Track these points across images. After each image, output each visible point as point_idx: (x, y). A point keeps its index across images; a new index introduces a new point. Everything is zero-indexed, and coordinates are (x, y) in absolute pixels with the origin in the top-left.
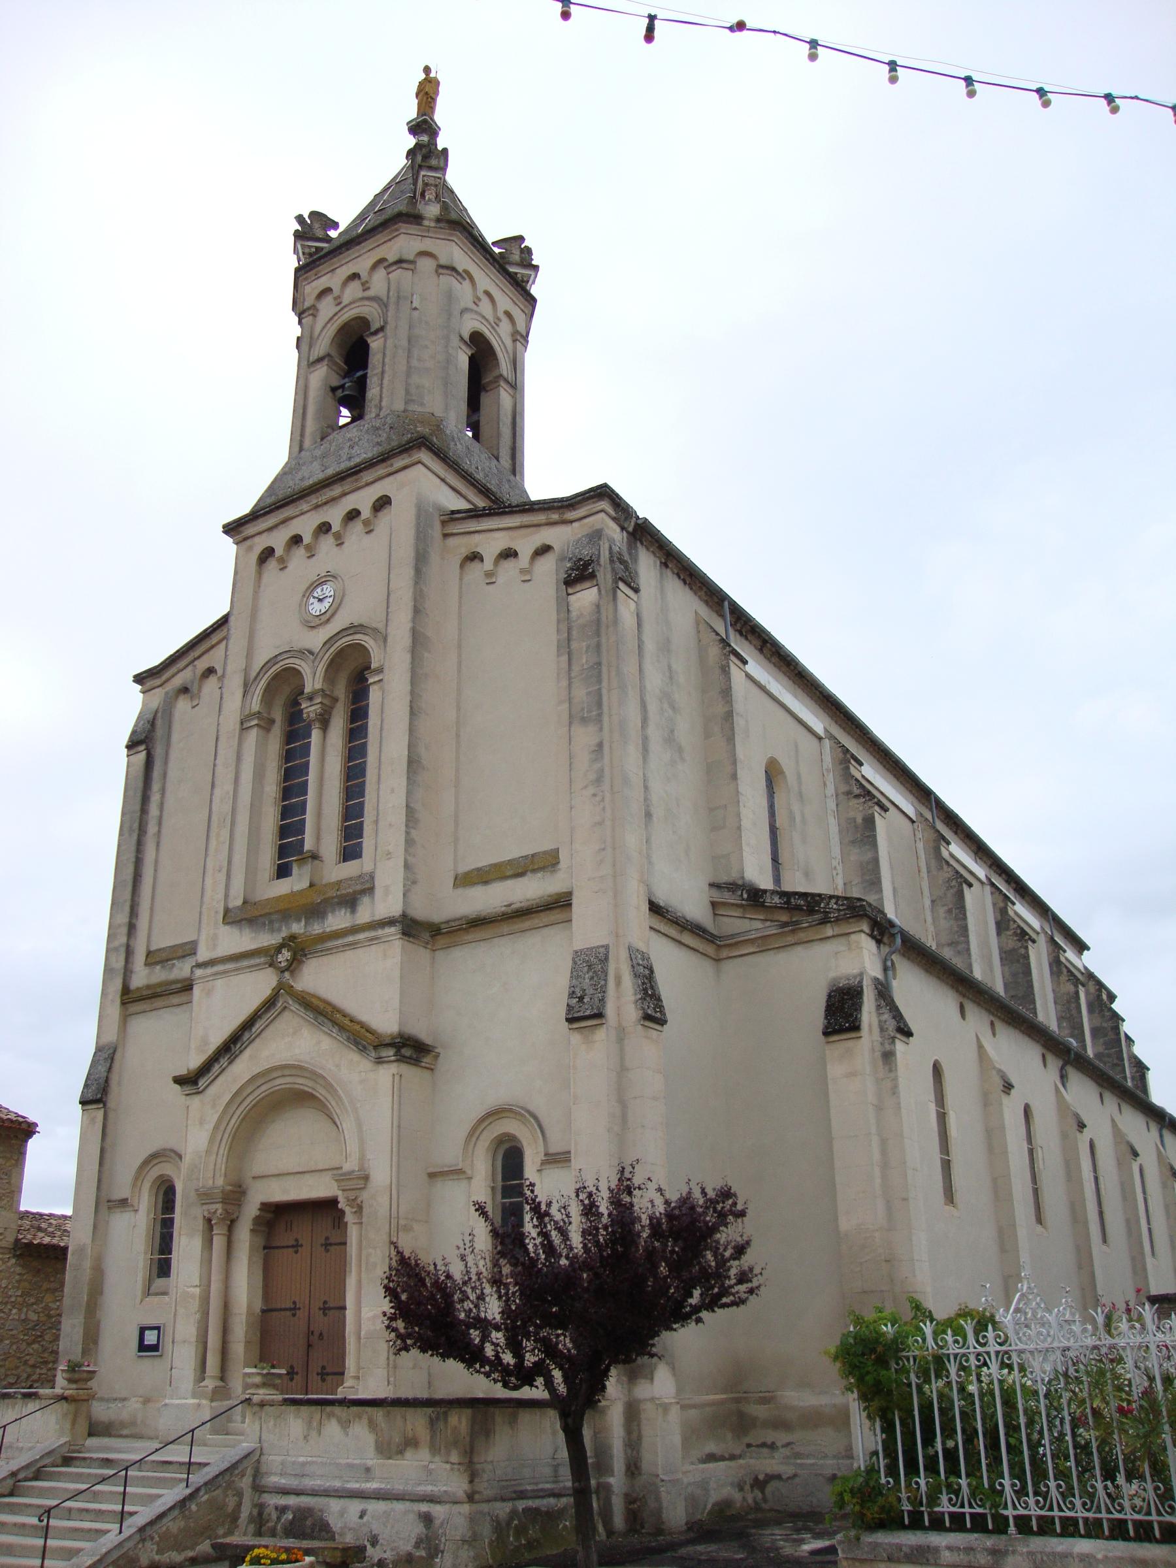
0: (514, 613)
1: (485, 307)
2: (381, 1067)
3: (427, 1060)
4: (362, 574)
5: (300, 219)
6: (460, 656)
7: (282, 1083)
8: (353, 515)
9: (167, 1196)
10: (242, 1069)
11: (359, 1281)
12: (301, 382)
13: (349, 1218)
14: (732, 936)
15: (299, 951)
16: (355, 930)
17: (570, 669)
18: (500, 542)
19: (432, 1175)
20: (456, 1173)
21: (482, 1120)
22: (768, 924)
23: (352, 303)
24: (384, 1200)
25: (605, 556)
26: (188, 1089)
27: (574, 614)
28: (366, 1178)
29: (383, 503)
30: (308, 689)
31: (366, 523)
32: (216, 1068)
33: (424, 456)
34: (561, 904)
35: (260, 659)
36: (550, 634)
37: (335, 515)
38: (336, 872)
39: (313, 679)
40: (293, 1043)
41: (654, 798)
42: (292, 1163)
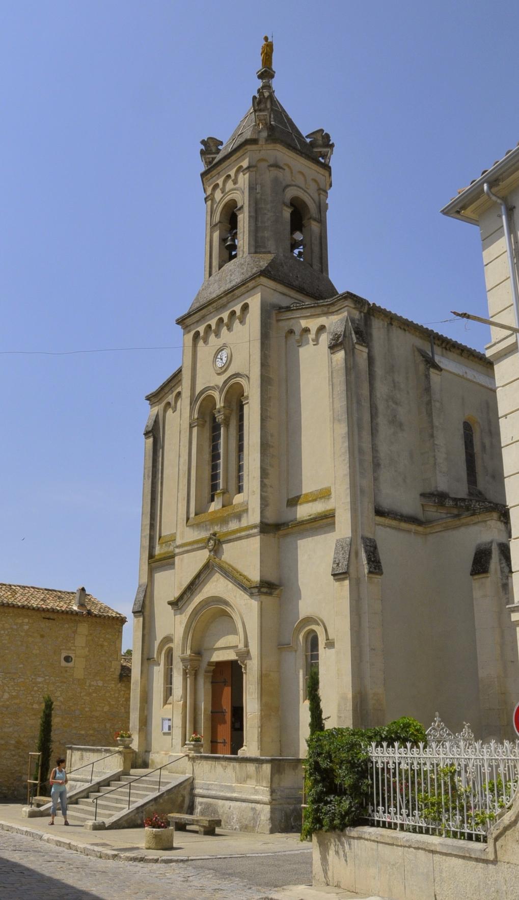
3: (277, 592)
5: (203, 142)
10: (197, 599)
27: (334, 364)
32: (185, 597)
40: (217, 586)
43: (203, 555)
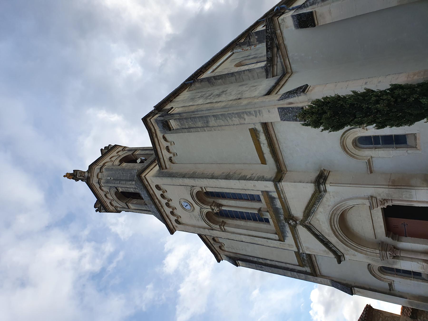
0: (185, 146)
1: (113, 159)
2: (327, 190)
4: (177, 193)
5: (96, 211)
6: (198, 163)
7: (337, 226)
8: (163, 196)
9: (384, 270)
10: (333, 240)
11: (415, 201)
12: (134, 211)
13: (390, 204)
14: (283, 68)
15: (289, 217)
16: (280, 198)
17: (194, 128)
18: (165, 152)
19: (371, 172)
20: (369, 163)
21: (347, 153)
22: (278, 55)
23: (112, 196)
24: (381, 190)
25: (162, 118)
26: (342, 259)
27: (179, 127)
28: (372, 197)
29: (158, 187)
30: (211, 211)
31: (163, 192)
33: (143, 175)
34: (265, 126)
35: (204, 224)
36: (185, 135)
37: (164, 202)
38: (263, 205)
39: (207, 209)
41: (234, 98)
42: (370, 223)
43: (302, 231)
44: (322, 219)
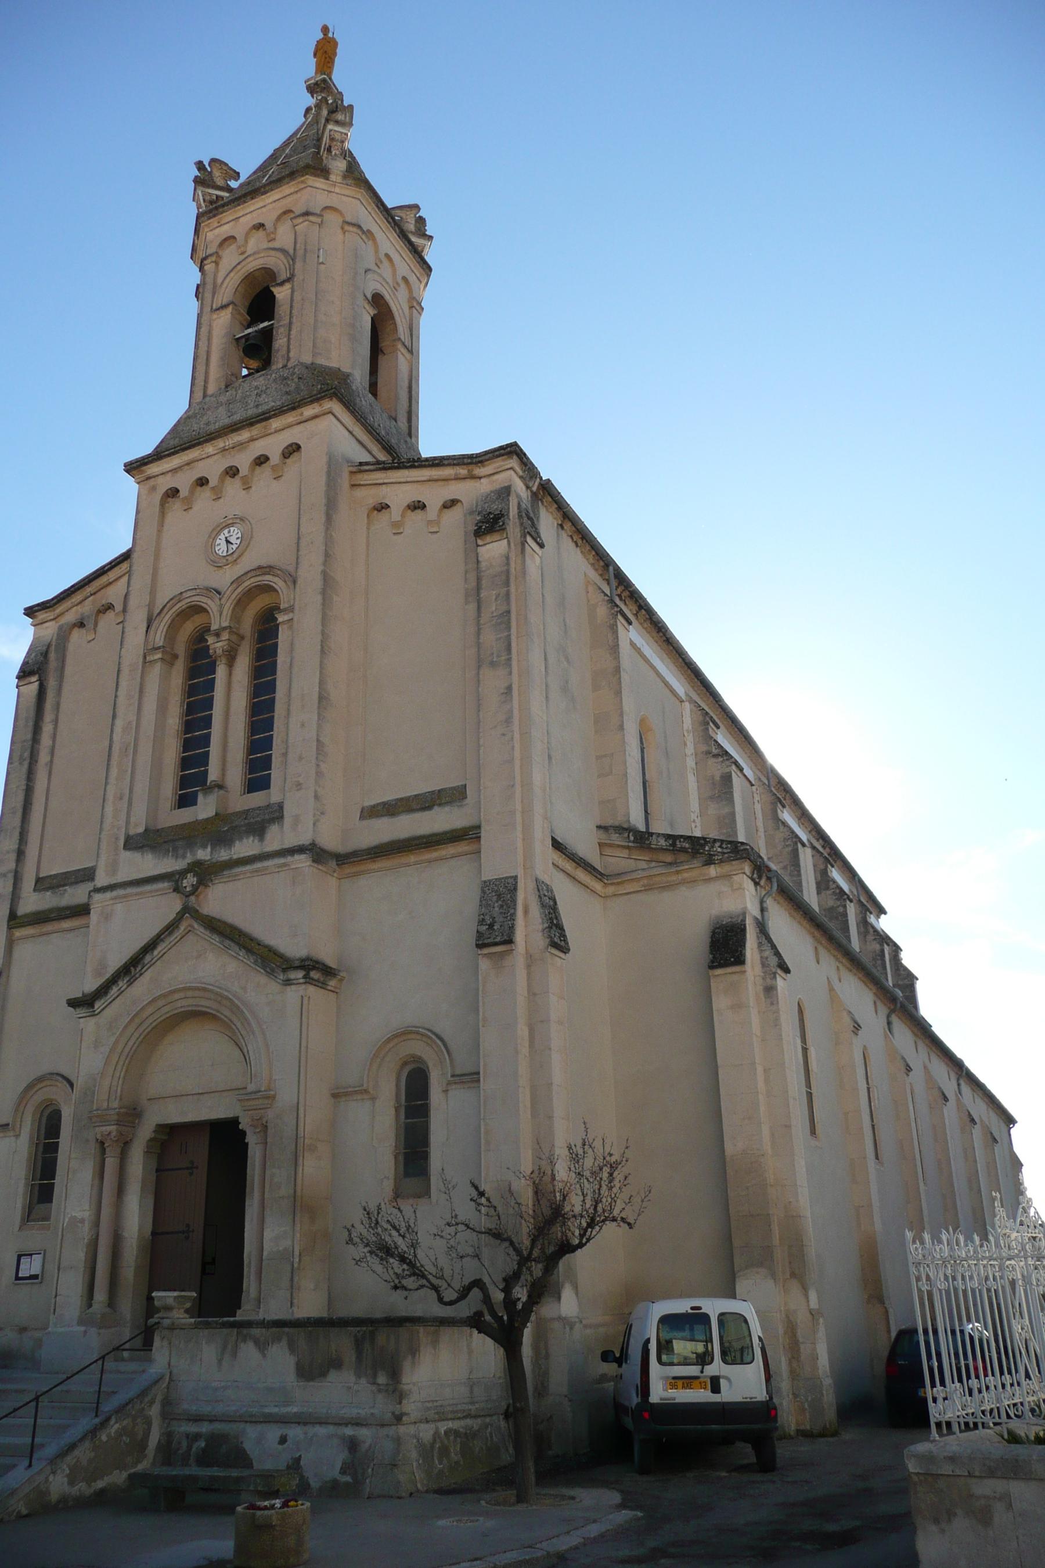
1: (386, 270)
3: (332, 983)
5: (200, 165)
8: (261, 460)
22: (653, 864)
23: (257, 253)
26: (82, 1012)
27: (483, 565)
29: (294, 449)
30: (214, 627)
31: (274, 468)
32: (114, 991)
37: (243, 461)
38: (240, 801)
39: (219, 617)
43: (162, 907)
44: (199, 965)
